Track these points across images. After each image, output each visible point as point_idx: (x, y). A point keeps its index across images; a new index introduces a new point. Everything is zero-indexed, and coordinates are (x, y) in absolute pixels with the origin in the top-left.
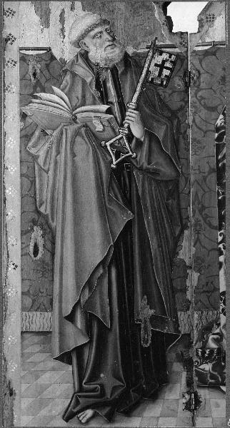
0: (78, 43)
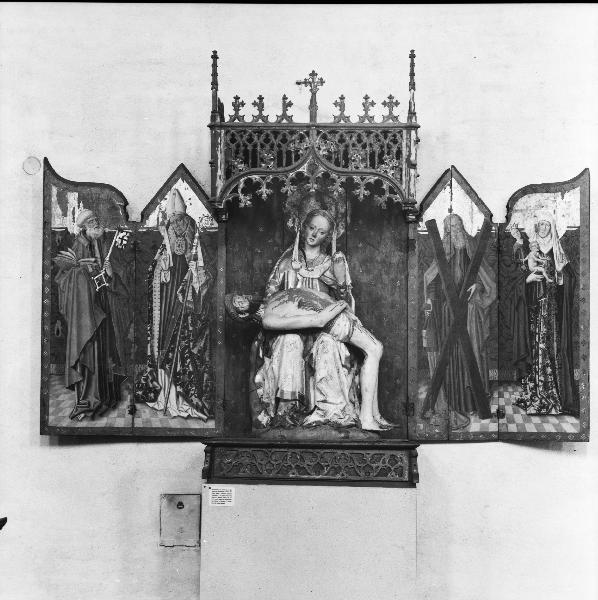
0: (81, 226)
